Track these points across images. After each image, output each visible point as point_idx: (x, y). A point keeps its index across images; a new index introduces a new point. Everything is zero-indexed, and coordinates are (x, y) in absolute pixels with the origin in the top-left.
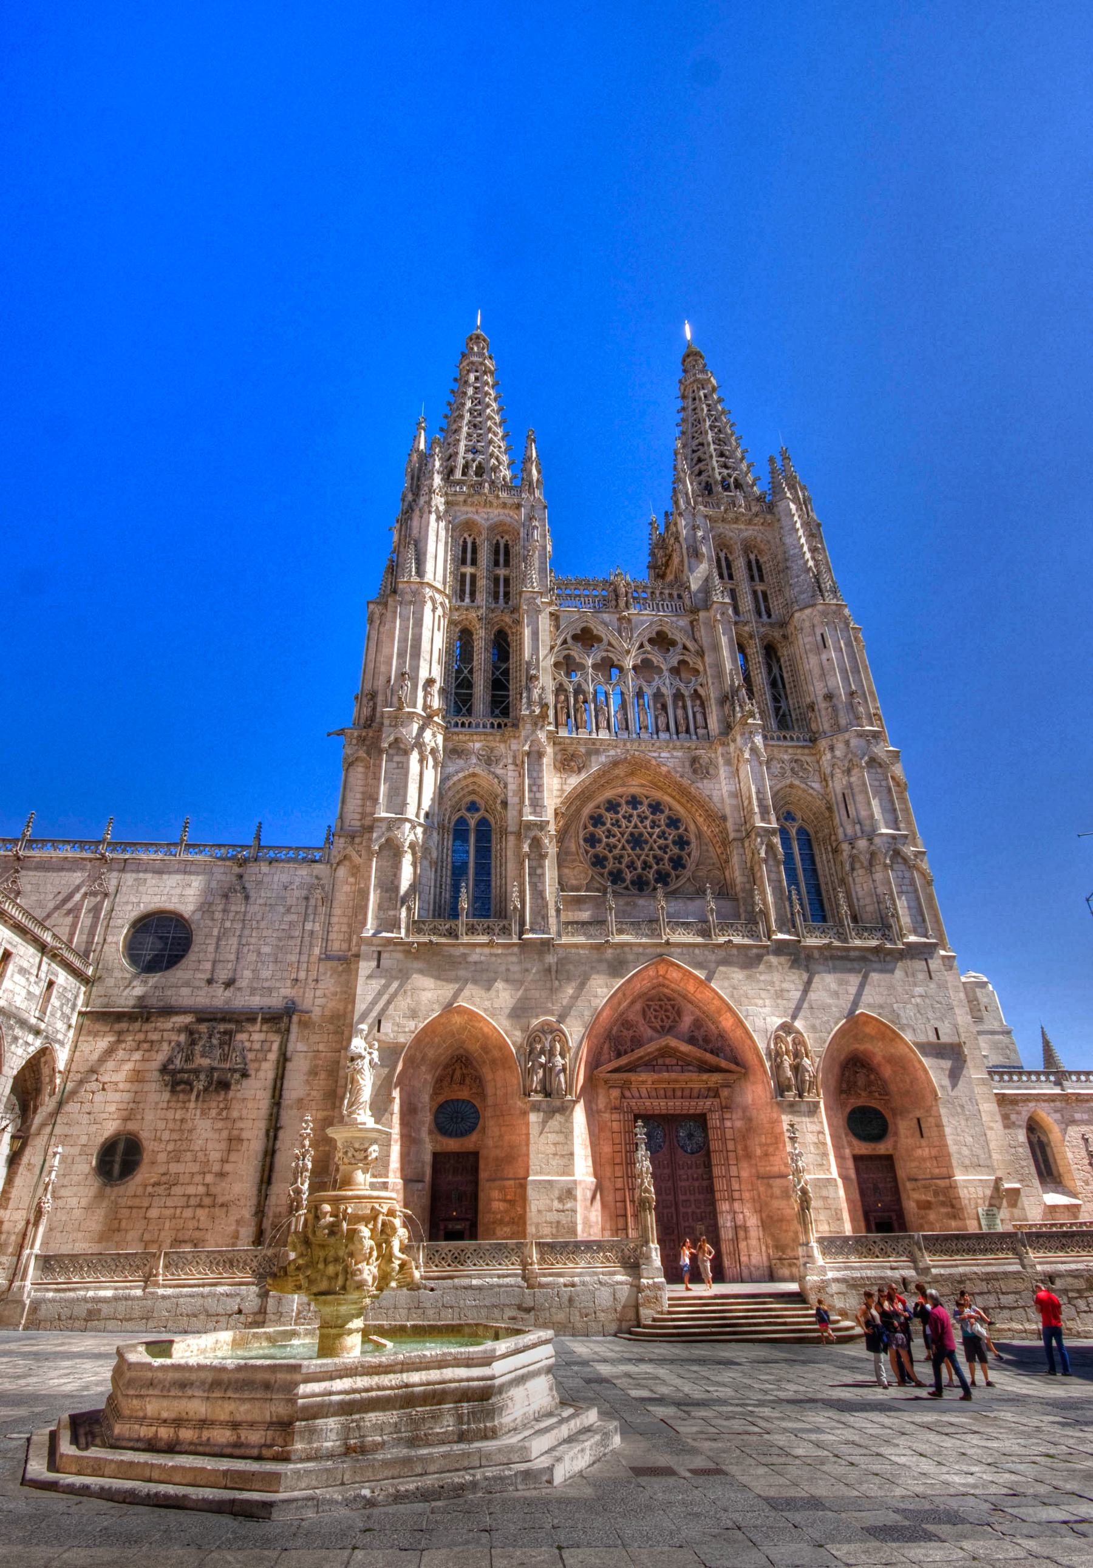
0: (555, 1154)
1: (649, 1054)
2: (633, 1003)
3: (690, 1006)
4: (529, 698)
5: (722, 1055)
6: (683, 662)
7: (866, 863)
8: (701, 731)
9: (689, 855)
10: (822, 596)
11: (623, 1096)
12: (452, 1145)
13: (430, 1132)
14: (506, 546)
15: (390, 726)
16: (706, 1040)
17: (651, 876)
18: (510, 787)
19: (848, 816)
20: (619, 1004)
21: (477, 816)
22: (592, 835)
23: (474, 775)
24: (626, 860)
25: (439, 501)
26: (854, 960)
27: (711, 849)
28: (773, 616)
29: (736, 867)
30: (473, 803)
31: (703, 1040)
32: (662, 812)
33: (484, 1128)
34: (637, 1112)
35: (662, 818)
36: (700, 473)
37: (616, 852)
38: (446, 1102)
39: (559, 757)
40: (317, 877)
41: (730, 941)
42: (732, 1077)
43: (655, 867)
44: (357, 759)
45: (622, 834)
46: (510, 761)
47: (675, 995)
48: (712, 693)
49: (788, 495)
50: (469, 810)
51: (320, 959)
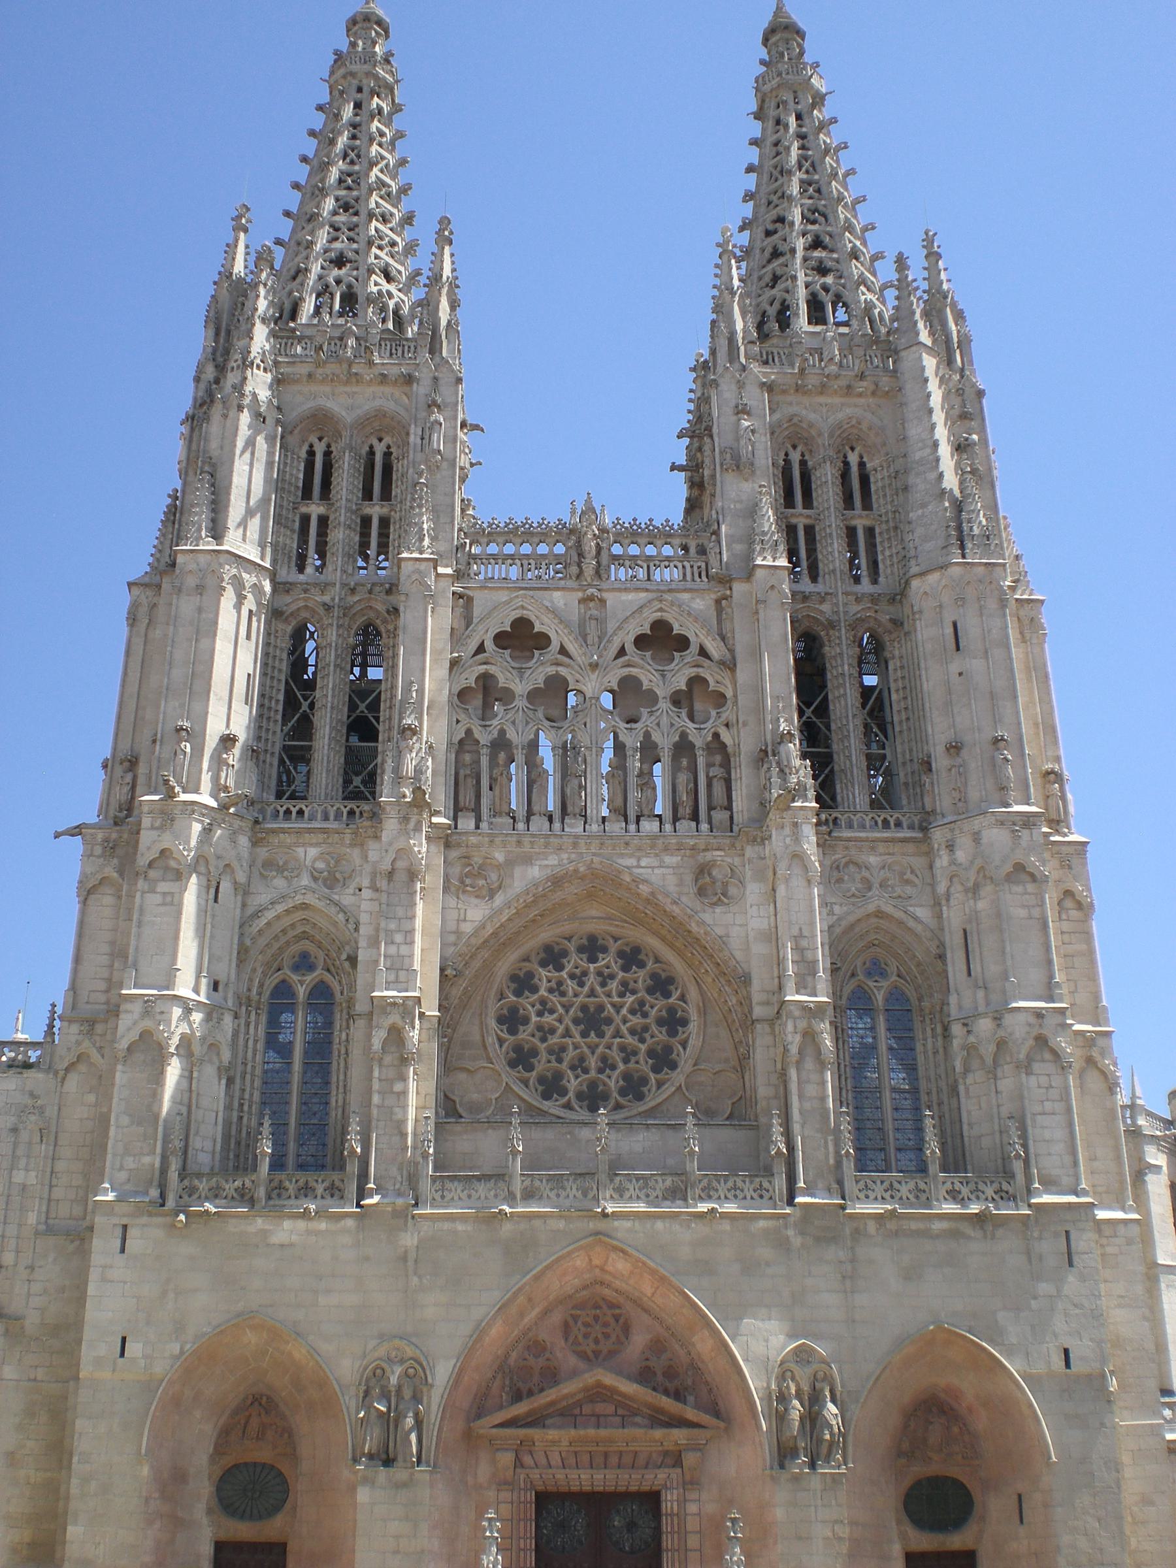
0: (397, 1552)
1: (566, 1397)
2: (546, 1312)
3: (645, 1317)
4: (397, 770)
5: (691, 1399)
6: (697, 682)
7: (989, 1061)
8: (719, 816)
9: (684, 1044)
10: (962, 547)
11: (518, 1463)
12: (243, 1531)
13: (209, 1512)
14: (387, 454)
15: (153, 828)
16: (670, 1373)
17: (612, 1084)
18: (362, 930)
19: (969, 974)
20: (522, 1315)
21: (309, 978)
22: (514, 1010)
23: (305, 906)
24: (570, 1055)
25: (259, 384)
26: (938, 1236)
27: (724, 1033)
28: (881, 579)
29: (759, 1069)
30: (305, 956)
31: (664, 1374)
32: (641, 965)
33: (294, 1508)
34: (541, 1488)
35: (641, 976)
36: (776, 279)
37: (554, 1040)
38: (236, 1466)
39: (456, 870)
40: (32, 1095)
41: (713, 1210)
42: (707, 1434)
43: (621, 1067)
44: (103, 881)
45: (567, 1008)
46: (366, 882)
47: (621, 1300)
48: (744, 743)
49: (924, 337)
50: (296, 968)
51: (37, 1233)
